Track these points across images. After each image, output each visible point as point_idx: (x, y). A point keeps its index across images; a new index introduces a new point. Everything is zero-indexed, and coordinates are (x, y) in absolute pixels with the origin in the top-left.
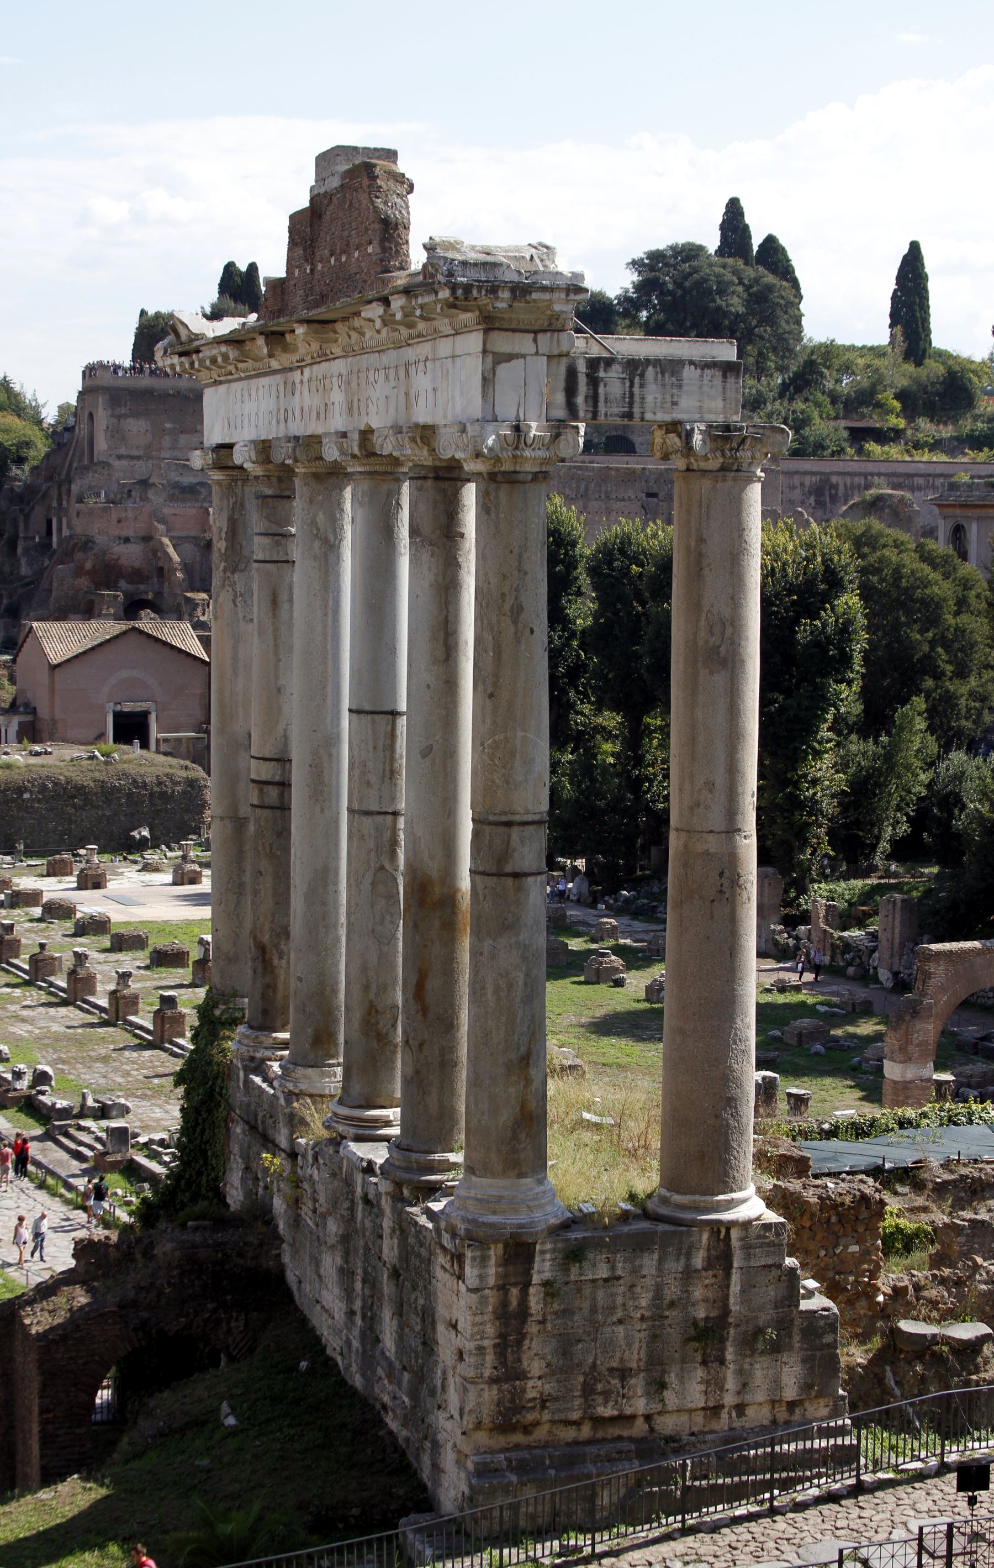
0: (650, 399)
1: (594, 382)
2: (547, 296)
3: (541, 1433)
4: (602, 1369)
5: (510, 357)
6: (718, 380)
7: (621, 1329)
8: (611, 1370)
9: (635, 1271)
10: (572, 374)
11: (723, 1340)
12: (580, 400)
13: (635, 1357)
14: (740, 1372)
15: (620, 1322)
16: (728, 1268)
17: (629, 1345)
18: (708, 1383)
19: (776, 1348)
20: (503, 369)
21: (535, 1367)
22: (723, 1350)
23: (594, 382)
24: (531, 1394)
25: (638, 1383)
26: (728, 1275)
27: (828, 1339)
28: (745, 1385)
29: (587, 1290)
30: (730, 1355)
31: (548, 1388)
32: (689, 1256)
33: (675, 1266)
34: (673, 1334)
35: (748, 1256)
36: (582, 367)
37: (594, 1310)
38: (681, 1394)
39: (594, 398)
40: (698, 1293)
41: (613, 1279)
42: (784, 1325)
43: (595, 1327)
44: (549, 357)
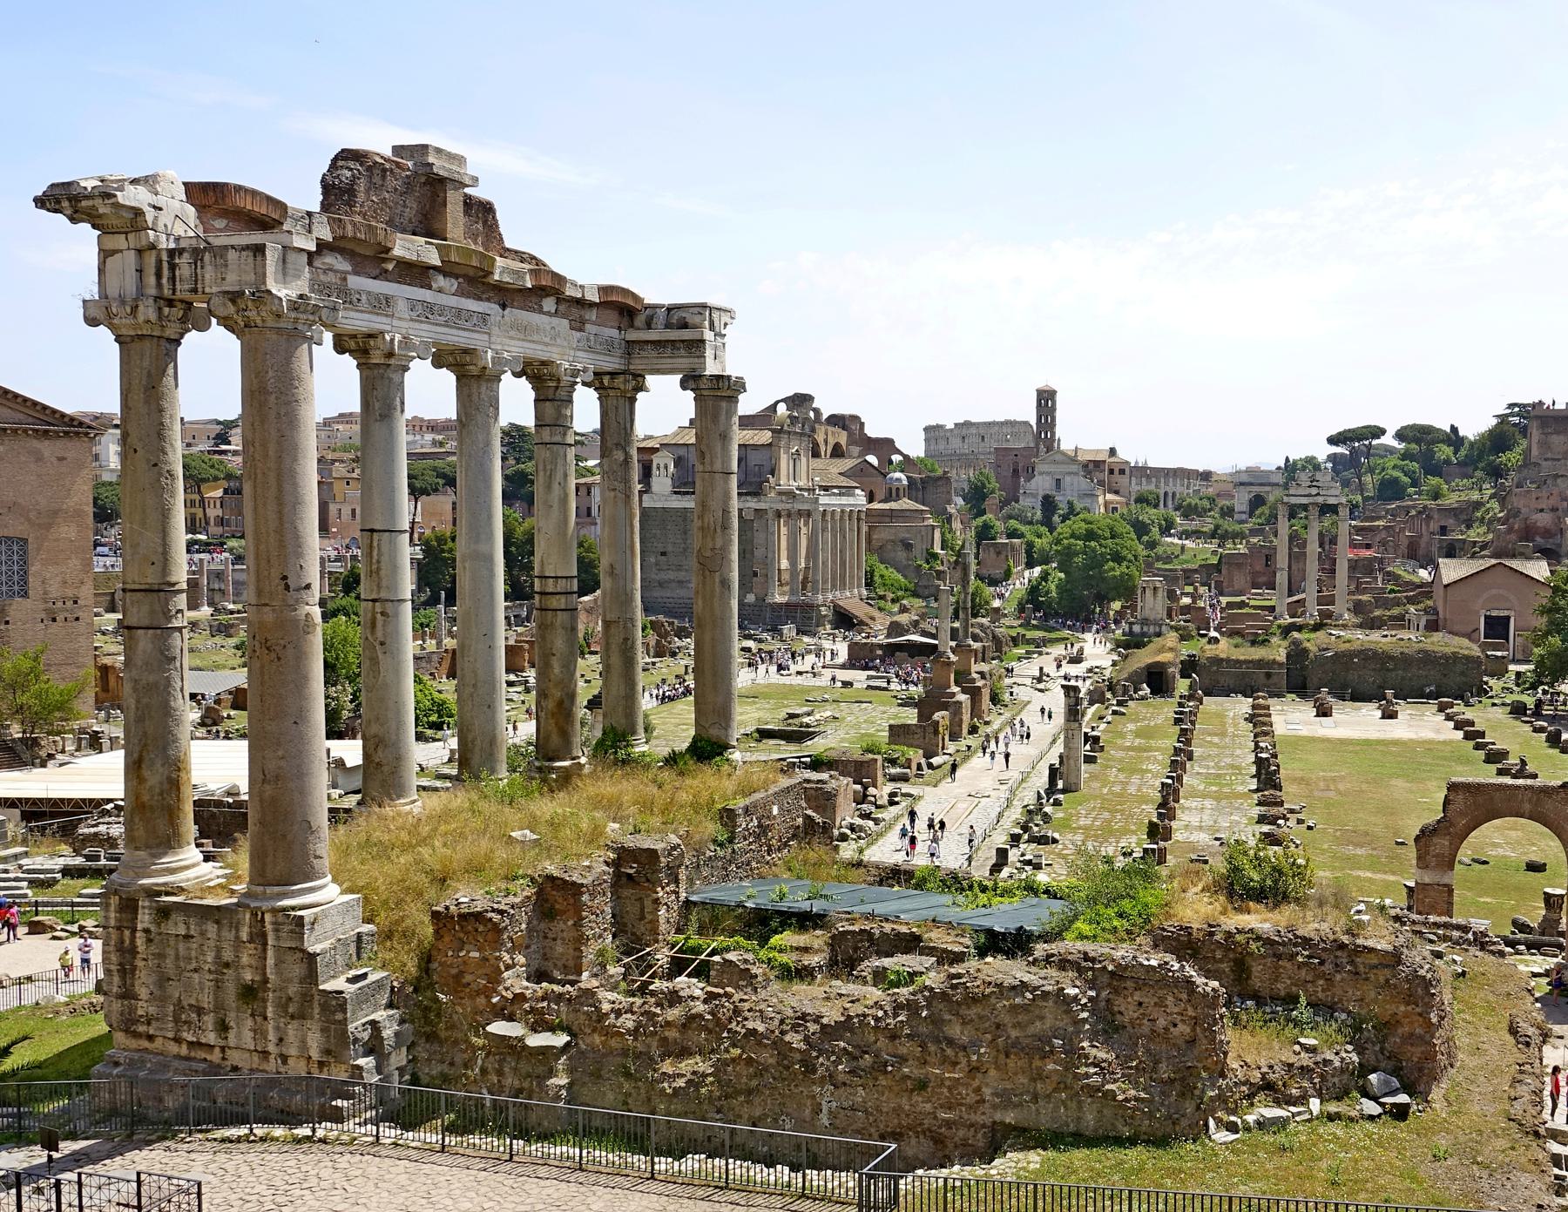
0: (207, 276)
1: (173, 267)
2: (90, 203)
3: (159, 1042)
4: (185, 1003)
5: (114, 252)
6: (251, 259)
7: (196, 976)
8: (191, 1006)
9: (203, 933)
10: (159, 262)
11: (265, 1001)
12: (164, 281)
13: (206, 1001)
14: (277, 1028)
15: (196, 970)
16: (265, 944)
17: (202, 989)
18: (255, 1031)
19: (301, 1016)
20: (109, 260)
21: (143, 993)
22: (265, 1008)
23: (173, 267)
24: (140, 1012)
25: (209, 1020)
26: (265, 950)
27: (339, 1016)
28: (281, 1040)
29: (172, 943)
30: (269, 1015)
31: (152, 1010)
32: (237, 931)
33: (228, 935)
34: (231, 990)
35: (278, 938)
36: (165, 257)
37: (177, 957)
38: (239, 1036)
39: (173, 279)
40: (245, 959)
41: (187, 937)
42: (306, 998)
43: (180, 971)
44: (140, 252)
